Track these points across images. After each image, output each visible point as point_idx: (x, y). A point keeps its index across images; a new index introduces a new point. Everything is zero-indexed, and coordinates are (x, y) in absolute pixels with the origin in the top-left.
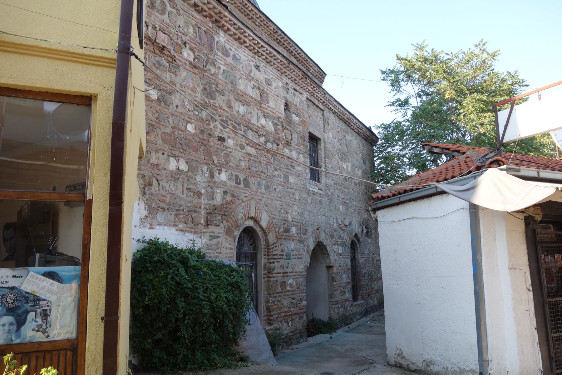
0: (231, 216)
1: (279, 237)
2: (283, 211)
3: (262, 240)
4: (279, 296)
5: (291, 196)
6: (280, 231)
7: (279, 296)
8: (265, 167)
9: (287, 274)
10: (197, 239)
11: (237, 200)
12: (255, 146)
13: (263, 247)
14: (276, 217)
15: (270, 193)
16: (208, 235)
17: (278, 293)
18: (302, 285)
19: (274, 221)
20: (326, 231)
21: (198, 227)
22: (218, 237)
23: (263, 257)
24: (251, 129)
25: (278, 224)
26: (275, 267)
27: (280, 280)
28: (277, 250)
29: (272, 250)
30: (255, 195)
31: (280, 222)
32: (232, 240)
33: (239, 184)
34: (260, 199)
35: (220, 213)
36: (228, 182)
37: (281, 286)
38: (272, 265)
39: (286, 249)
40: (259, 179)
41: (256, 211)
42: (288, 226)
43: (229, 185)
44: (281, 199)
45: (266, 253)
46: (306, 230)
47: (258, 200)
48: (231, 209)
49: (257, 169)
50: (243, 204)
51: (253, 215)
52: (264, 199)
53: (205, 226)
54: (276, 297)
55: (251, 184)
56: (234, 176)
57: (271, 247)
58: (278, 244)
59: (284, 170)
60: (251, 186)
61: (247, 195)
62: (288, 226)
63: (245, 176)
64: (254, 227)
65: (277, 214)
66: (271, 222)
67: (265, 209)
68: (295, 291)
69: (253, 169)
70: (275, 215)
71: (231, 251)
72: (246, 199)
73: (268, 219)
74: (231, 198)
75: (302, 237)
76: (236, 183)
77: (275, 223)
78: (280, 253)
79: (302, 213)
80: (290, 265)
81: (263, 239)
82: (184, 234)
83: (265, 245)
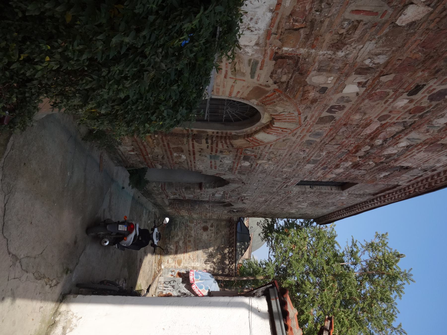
0: (282, 97)
1: (240, 150)
2: (272, 156)
3: (238, 131)
4: (164, 145)
5: (288, 165)
6: (246, 151)
7: (164, 145)
8: (339, 143)
9: (192, 154)
10: (256, 37)
11: (304, 106)
12: (373, 136)
13: (229, 132)
14: (266, 149)
15: (300, 145)
16: (258, 57)
17: (168, 144)
18: (179, 166)
19: (262, 147)
20: (240, 188)
21: (278, 41)
22: (253, 74)
23: (215, 131)
24: (403, 130)
25: (257, 151)
26: (201, 143)
27: (185, 147)
28: (223, 147)
29: (224, 142)
30: (304, 129)
31: (260, 152)
32: (245, 95)
33: (330, 111)
34: (296, 133)
35: (293, 79)
36: (339, 95)
37: (178, 148)
38: (204, 141)
39: (224, 156)
40: (325, 135)
41: (281, 128)
42: (252, 159)
43: (333, 96)
44: (288, 155)
45: (220, 135)
46: (244, 174)
47: (295, 132)
48: (294, 97)
49: (341, 134)
50: (296, 114)
51: (276, 124)
52: (294, 139)
53: (276, 53)
54: (163, 141)
55: (322, 126)
56: (345, 104)
57: (228, 141)
58: (231, 148)
59: (325, 161)
60: (320, 125)
61: (308, 119)
62: (252, 159)
63: (337, 118)
64: (258, 124)
65: (270, 150)
66: (261, 143)
67: (280, 139)
68: (173, 160)
69: (344, 129)
70: (270, 148)
71: (227, 93)
72: (303, 118)
73: (266, 141)
74: (310, 98)
75: (236, 170)
76: (332, 107)
77: (259, 148)
78: (219, 150)
79: (264, 172)
80: (203, 158)
81: (240, 133)
82: (271, 11)
83: (231, 134)
